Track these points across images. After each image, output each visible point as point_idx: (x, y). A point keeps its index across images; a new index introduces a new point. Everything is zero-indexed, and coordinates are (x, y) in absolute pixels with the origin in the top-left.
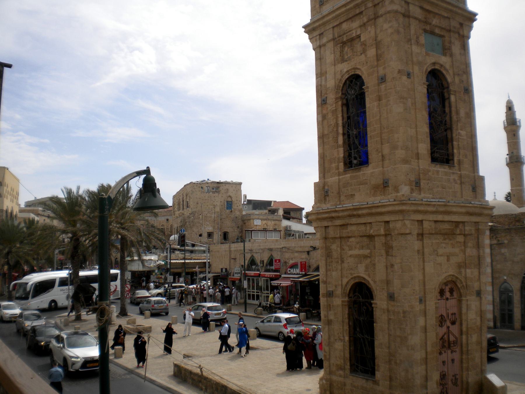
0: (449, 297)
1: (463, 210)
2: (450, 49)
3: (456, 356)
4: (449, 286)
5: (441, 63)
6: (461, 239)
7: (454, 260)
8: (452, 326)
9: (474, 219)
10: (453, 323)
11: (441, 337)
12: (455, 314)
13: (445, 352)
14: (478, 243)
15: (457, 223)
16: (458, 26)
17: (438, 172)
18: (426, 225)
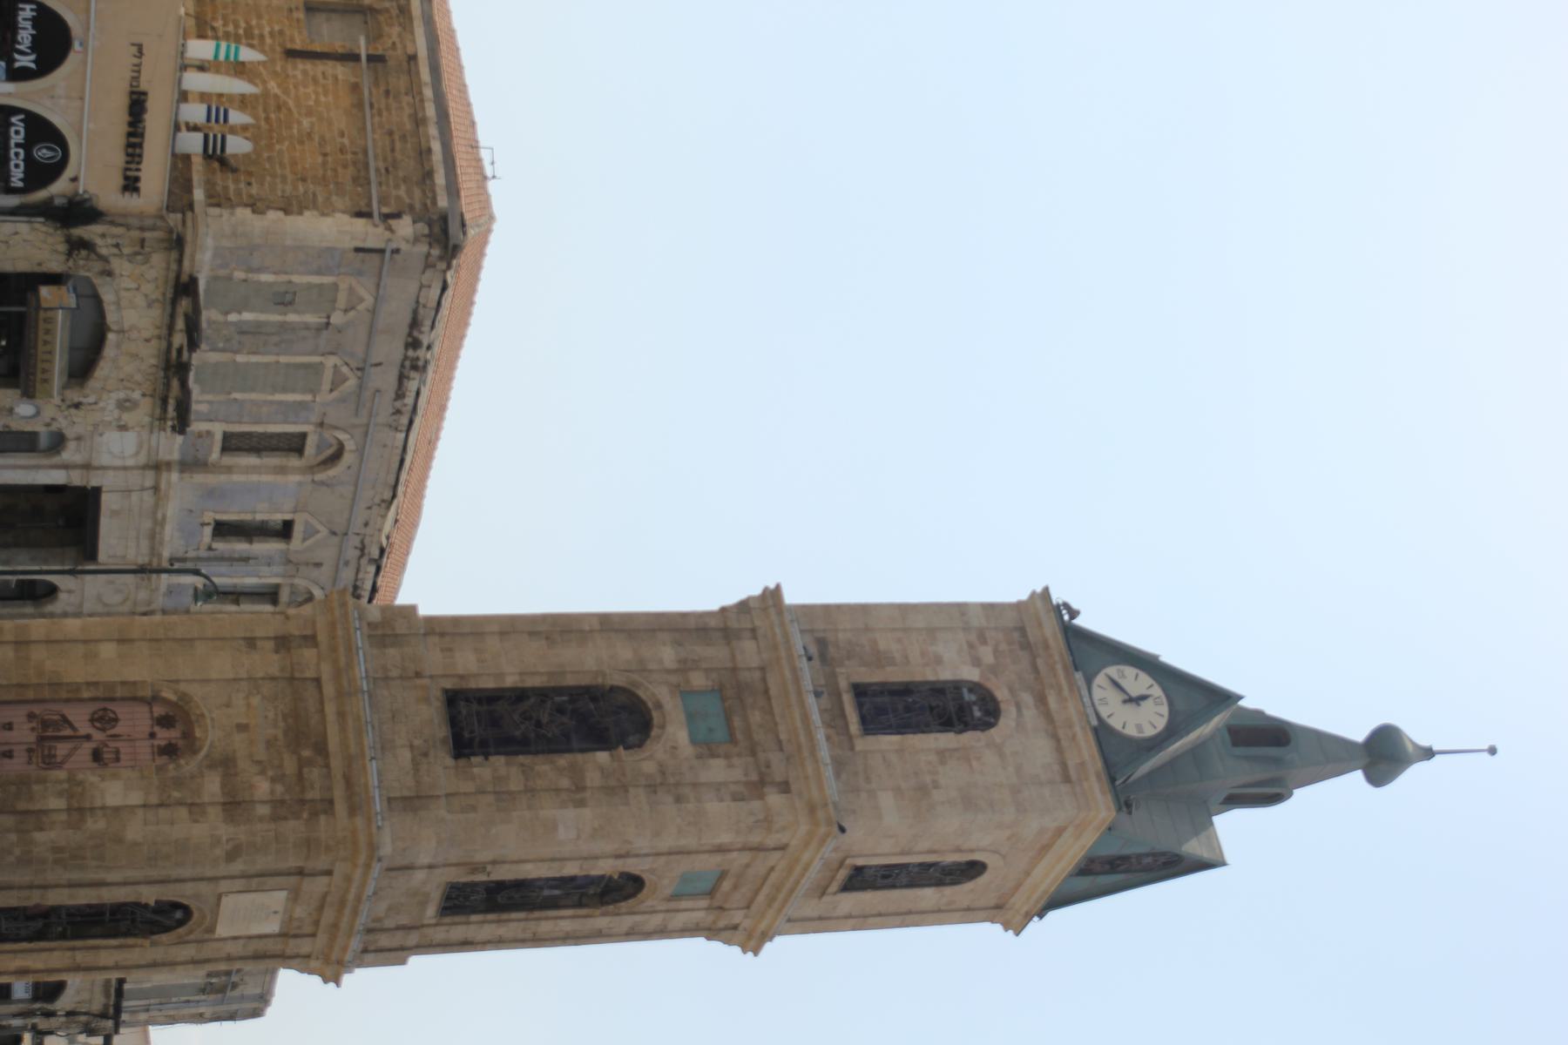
0: (156, 742)
1: (353, 749)
2: (713, 755)
3: (17, 765)
4: (181, 743)
5: (670, 729)
6: (290, 766)
7: (239, 741)
8: (89, 751)
9: (338, 793)
10: (97, 756)
11: (70, 718)
12: (118, 760)
13: (33, 729)
14: (285, 818)
15: (321, 749)
16: (778, 779)
17: (427, 700)
18: (309, 654)
